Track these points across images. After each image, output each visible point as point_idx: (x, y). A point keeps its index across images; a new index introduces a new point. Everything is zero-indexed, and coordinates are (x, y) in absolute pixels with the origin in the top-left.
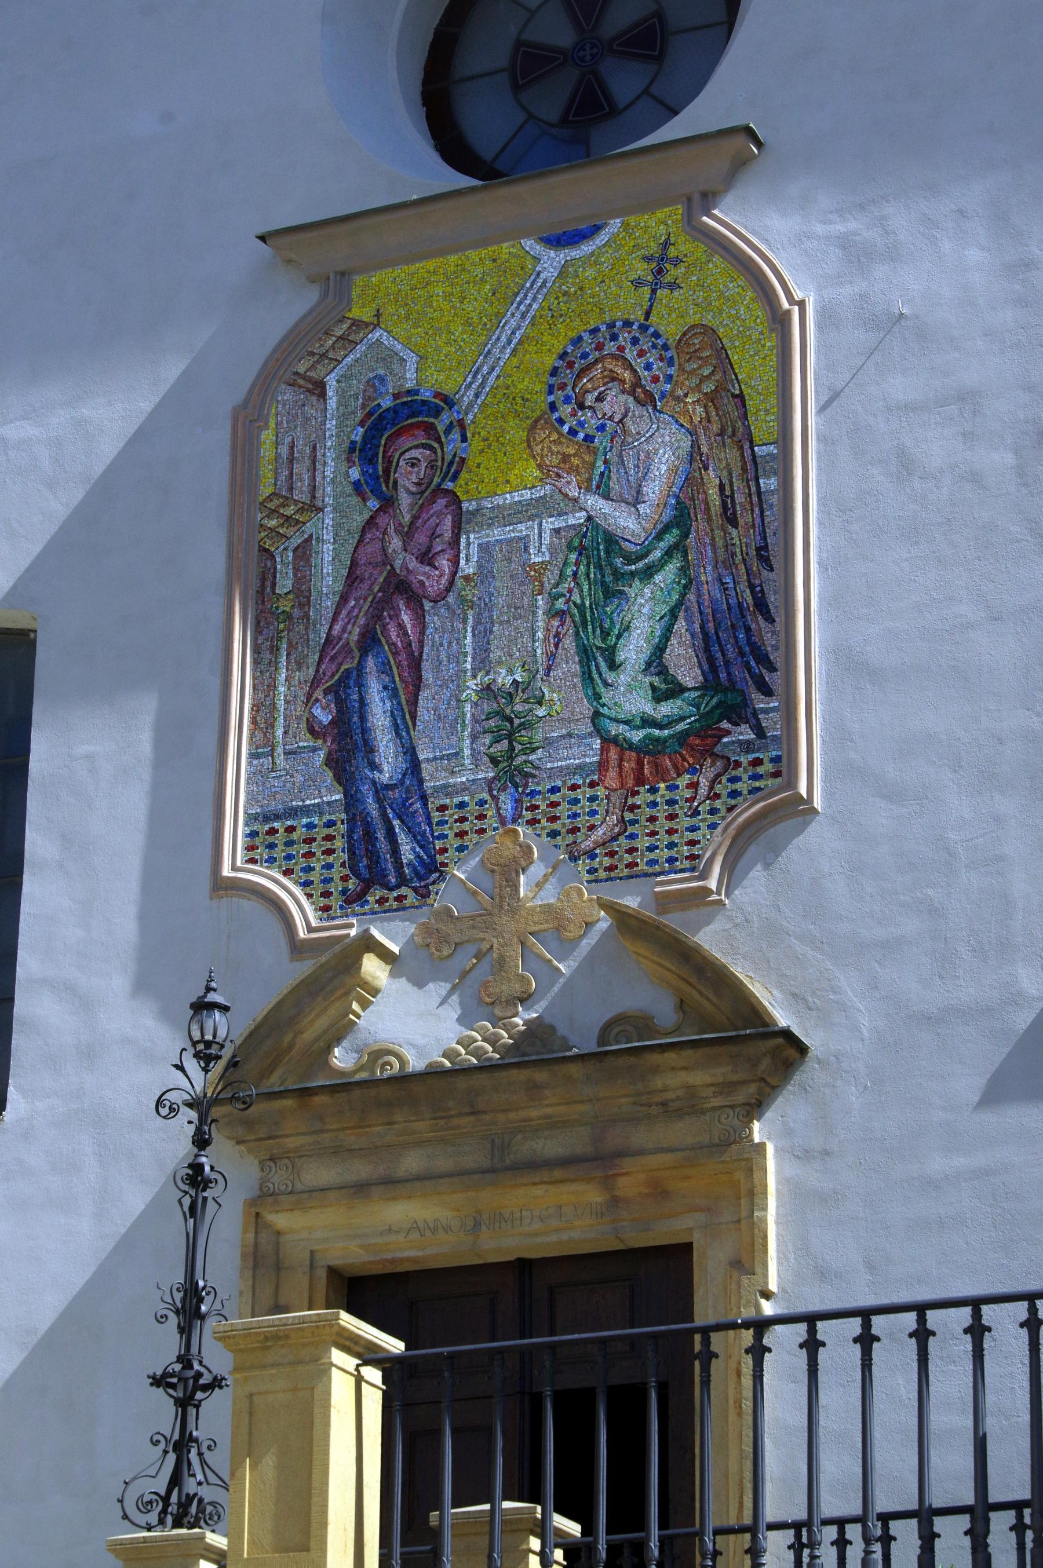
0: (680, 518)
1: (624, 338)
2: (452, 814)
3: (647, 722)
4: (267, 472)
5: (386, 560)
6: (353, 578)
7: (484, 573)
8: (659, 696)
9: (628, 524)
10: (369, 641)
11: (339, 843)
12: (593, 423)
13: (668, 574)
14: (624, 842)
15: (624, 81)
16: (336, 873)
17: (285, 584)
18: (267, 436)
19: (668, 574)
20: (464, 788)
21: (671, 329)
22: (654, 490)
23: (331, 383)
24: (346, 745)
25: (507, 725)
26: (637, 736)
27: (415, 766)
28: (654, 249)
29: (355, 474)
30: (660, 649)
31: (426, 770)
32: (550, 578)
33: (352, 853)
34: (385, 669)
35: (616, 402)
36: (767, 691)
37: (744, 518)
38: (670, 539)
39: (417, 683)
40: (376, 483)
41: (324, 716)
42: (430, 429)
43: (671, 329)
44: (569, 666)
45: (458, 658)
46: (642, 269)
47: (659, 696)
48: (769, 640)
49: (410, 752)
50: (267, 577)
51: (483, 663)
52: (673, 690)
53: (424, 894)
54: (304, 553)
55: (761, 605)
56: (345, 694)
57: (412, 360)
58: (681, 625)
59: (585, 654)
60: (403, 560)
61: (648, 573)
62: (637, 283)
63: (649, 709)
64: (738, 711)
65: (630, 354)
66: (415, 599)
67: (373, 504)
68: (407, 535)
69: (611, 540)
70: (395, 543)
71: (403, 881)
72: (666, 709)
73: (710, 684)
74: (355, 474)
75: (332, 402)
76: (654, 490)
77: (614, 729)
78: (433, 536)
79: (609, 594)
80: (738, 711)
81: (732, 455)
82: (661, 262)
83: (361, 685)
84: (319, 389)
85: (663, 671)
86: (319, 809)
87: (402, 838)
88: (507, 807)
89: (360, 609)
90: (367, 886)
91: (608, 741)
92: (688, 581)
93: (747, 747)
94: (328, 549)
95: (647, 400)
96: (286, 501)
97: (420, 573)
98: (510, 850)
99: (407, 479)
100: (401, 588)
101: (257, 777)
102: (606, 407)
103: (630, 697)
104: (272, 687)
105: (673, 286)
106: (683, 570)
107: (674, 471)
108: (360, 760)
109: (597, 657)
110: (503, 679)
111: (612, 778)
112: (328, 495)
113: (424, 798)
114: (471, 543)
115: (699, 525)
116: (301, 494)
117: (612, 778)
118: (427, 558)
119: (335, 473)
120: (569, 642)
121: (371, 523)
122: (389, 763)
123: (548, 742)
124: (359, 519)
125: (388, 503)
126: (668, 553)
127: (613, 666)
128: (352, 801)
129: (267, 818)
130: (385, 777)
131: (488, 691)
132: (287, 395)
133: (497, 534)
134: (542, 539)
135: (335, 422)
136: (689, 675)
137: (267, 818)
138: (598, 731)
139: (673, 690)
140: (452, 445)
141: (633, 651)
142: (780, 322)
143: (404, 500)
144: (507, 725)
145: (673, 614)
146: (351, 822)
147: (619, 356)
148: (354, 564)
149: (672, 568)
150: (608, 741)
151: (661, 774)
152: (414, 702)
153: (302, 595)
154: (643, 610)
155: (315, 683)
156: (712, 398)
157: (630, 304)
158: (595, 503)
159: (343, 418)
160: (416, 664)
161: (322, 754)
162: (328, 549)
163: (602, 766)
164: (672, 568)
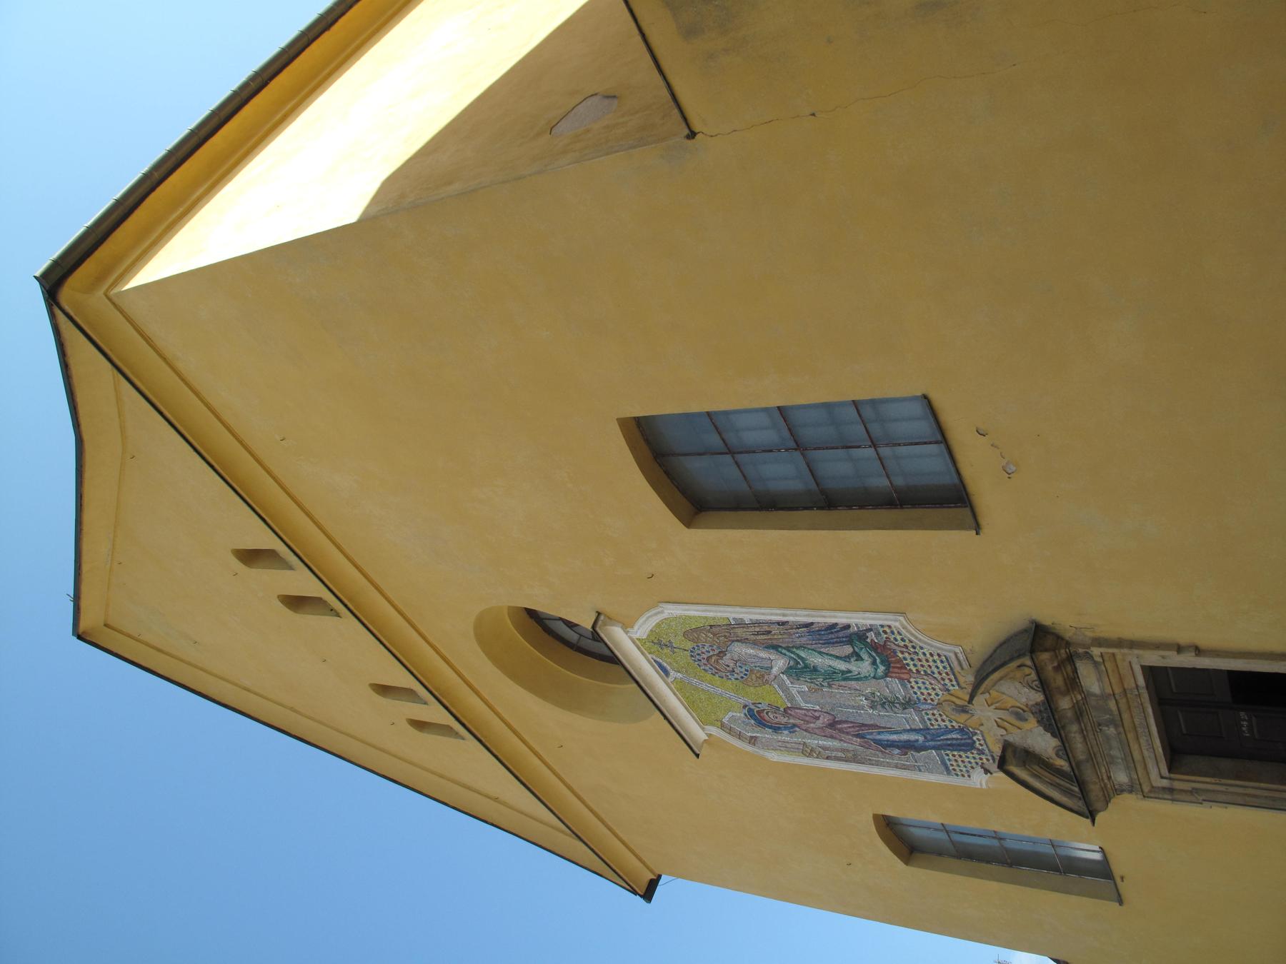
3: (874, 663)
6: (832, 737)
9: (780, 663)
14: (936, 675)
17: (840, 754)
41: (896, 751)
71: (971, 738)
72: (865, 656)
76: (763, 654)
91: (886, 675)
97: (825, 719)
100: (833, 724)
101: (930, 771)
103: (864, 667)
118: (817, 718)
129: (947, 768)
136: (848, 650)
137: (947, 768)
141: (842, 666)
145: (820, 653)
147: (708, 659)
150: (886, 675)
153: (843, 750)
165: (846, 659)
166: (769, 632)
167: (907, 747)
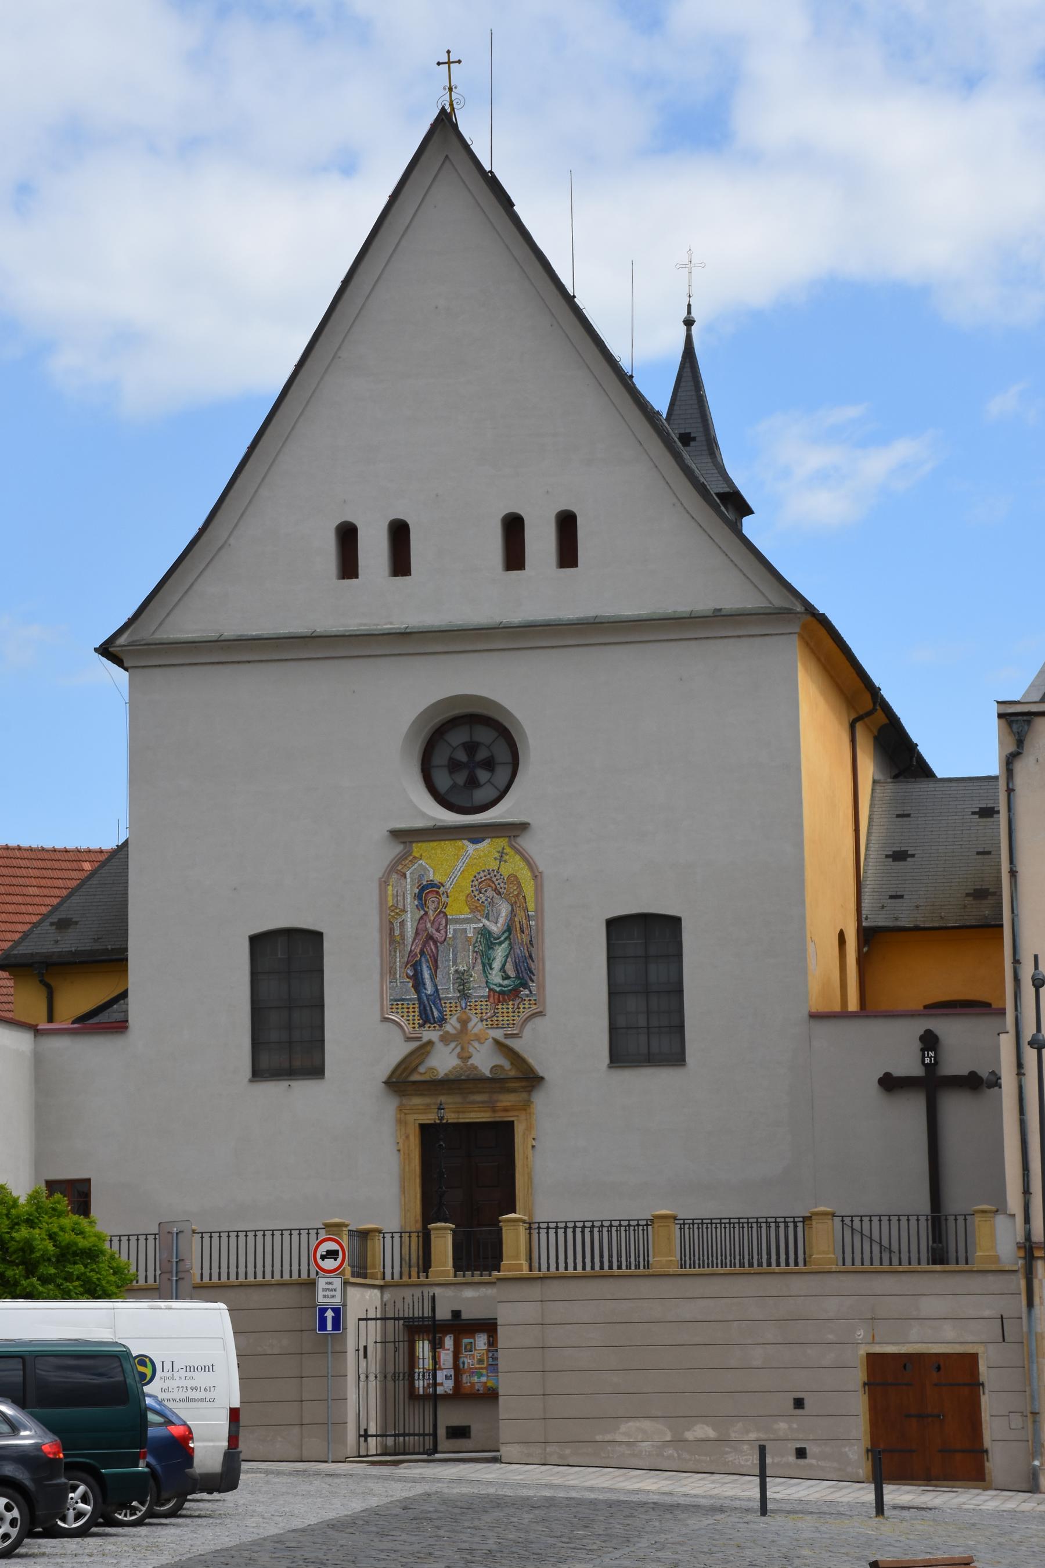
0: (509, 929)
1: (492, 875)
2: (448, 1005)
3: (501, 985)
4: (390, 899)
5: (426, 929)
6: (417, 933)
7: (454, 938)
8: (504, 979)
9: (495, 929)
10: (422, 953)
11: (417, 1010)
12: (484, 898)
13: (505, 945)
15: (483, 775)
16: (416, 1018)
17: (397, 932)
18: (390, 888)
19: (505, 945)
20: (451, 998)
21: (506, 875)
22: (501, 920)
23: (408, 874)
24: (418, 983)
25: (462, 980)
26: (498, 989)
27: (437, 990)
28: (500, 849)
29: (416, 903)
30: (504, 966)
31: (441, 992)
32: (473, 940)
33: (420, 1012)
34: (427, 961)
35: (490, 893)
36: (533, 981)
37: (526, 932)
38: (506, 935)
39: (436, 967)
40: (422, 905)
42: (438, 893)
43: (506, 875)
44: (479, 967)
45: (448, 961)
46: (497, 855)
47: (504, 979)
48: (533, 967)
49: (436, 986)
50: (392, 930)
51: (455, 963)
52: (507, 977)
53: (441, 1026)
54: (402, 924)
55: (531, 956)
56: (416, 966)
57: (431, 871)
58: (509, 959)
59: (484, 965)
60: (432, 930)
61: (500, 943)
62: (496, 859)
63: (501, 982)
64: (525, 986)
65: (494, 879)
66: (435, 942)
67: (422, 913)
68: (433, 923)
69: (489, 932)
70: (429, 925)
72: (506, 982)
73: (517, 977)
74: (416, 903)
75: (409, 880)
76: (501, 920)
77: (492, 987)
78: (440, 924)
79: (490, 948)
80: (525, 986)
81: (522, 913)
82: (502, 854)
83: (421, 966)
84: (404, 875)
85: (505, 972)
86: (410, 1000)
87: (434, 1010)
88: (463, 1005)
89: (419, 943)
90: (425, 1022)
91: (490, 990)
92: (511, 947)
93: (527, 996)
94: (409, 924)
95: (499, 894)
96: (397, 908)
97: (436, 935)
98: (464, 1017)
99: (432, 906)
102: (487, 894)
103: (496, 977)
104: (395, 962)
105: (506, 861)
106: (510, 944)
107: (507, 916)
108: (421, 987)
109: (487, 965)
110: (461, 969)
111: (491, 1000)
112: (409, 908)
113: (440, 1000)
114: (451, 928)
115: (514, 932)
116: (401, 906)
117: (491, 1000)
118: (438, 930)
119: (410, 902)
120: (479, 960)
121: (421, 918)
122: (430, 990)
123: (474, 988)
124: (418, 917)
125: (426, 913)
126: (506, 939)
127: (491, 969)
128: (419, 999)
129: (396, 1000)
130: (429, 993)
131: (456, 971)
132: (395, 876)
133: (458, 926)
134: (471, 930)
135: (410, 888)
136: (512, 974)
137: (396, 1000)
138: (488, 986)
139: (507, 977)
140: (444, 898)
141: (497, 965)
142: (537, 876)
143: (431, 913)
144: (462, 980)
145: (507, 956)
146: (419, 1004)
147: (490, 879)
148: (417, 929)
149: (507, 942)
150: (490, 990)
151: (504, 1000)
152: (436, 972)
153: (402, 935)
154: (499, 953)
155: (407, 963)
156: (517, 896)
157: (493, 865)
158: (485, 921)
159: (412, 885)
160: (436, 961)
161: (411, 985)
162: (409, 924)
163: (489, 996)
164: (507, 942)
165: (503, 969)
166: (523, 932)
167: (418, 983)
